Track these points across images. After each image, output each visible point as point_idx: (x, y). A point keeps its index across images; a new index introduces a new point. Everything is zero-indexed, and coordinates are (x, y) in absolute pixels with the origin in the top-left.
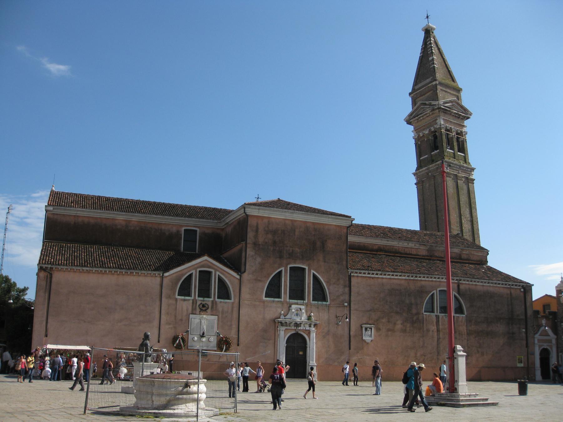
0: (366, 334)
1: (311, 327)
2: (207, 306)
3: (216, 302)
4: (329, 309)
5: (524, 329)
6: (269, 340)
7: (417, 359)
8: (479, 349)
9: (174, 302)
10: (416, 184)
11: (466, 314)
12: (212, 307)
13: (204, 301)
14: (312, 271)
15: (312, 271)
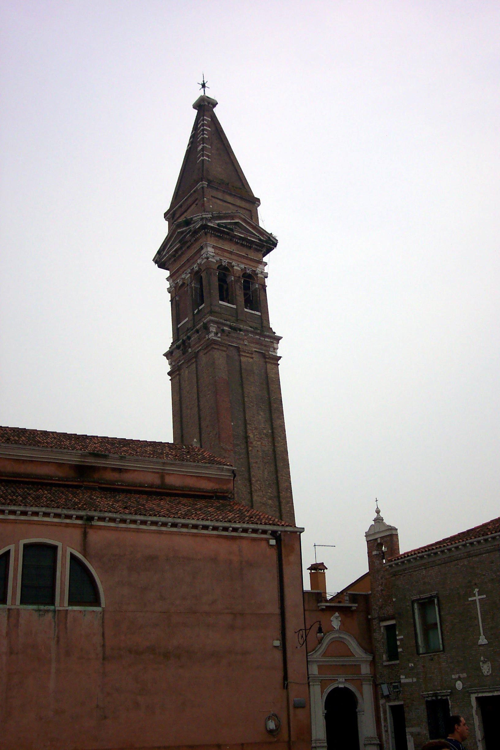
5: (277, 640)
10: (169, 374)
11: (103, 605)
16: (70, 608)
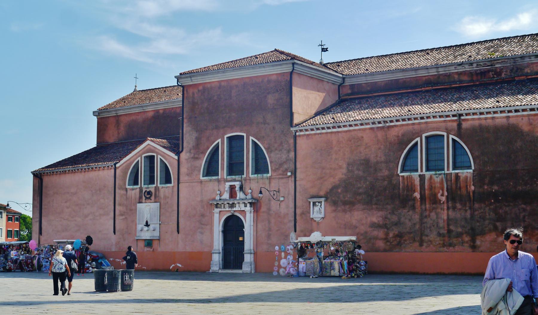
0: (315, 210)
1: (246, 207)
2: (151, 193)
3: (158, 187)
4: (270, 183)
6: (207, 225)
7: (388, 241)
8: (498, 224)
9: (125, 192)
12: (155, 194)
13: (148, 188)
14: (251, 138)
15: (251, 138)
16: (454, 171)
